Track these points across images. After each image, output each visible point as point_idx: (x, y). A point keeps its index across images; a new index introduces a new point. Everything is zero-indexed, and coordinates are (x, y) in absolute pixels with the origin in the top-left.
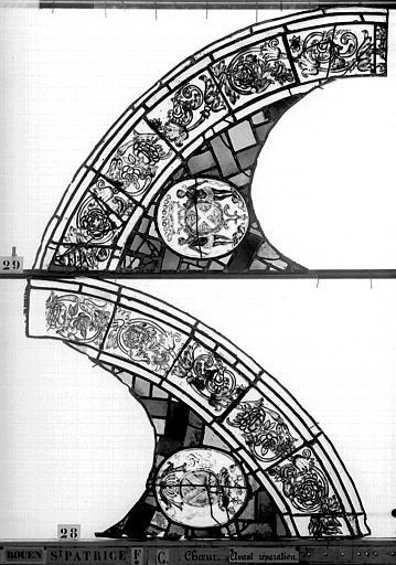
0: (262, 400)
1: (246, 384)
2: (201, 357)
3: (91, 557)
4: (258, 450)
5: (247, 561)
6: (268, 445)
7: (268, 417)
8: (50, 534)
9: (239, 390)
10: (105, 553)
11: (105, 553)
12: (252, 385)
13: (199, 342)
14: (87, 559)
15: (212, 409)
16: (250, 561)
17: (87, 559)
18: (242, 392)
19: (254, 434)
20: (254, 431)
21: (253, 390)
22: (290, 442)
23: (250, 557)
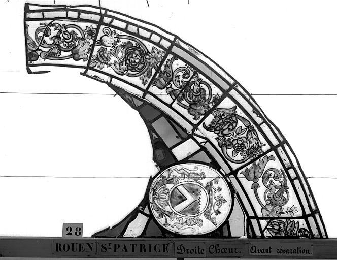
0: (236, 107)
1: (221, 93)
2: (179, 69)
3: (137, 248)
4: (230, 152)
5: (263, 254)
6: (240, 148)
7: (240, 123)
8: (57, 232)
9: (215, 99)
10: (150, 245)
11: (150, 245)
12: (226, 94)
13: (176, 57)
14: (133, 251)
15: (191, 118)
16: (269, 254)
17: (133, 251)
18: (218, 100)
19: (227, 138)
20: (226, 135)
21: (227, 99)
22: (259, 147)
23: (269, 251)
